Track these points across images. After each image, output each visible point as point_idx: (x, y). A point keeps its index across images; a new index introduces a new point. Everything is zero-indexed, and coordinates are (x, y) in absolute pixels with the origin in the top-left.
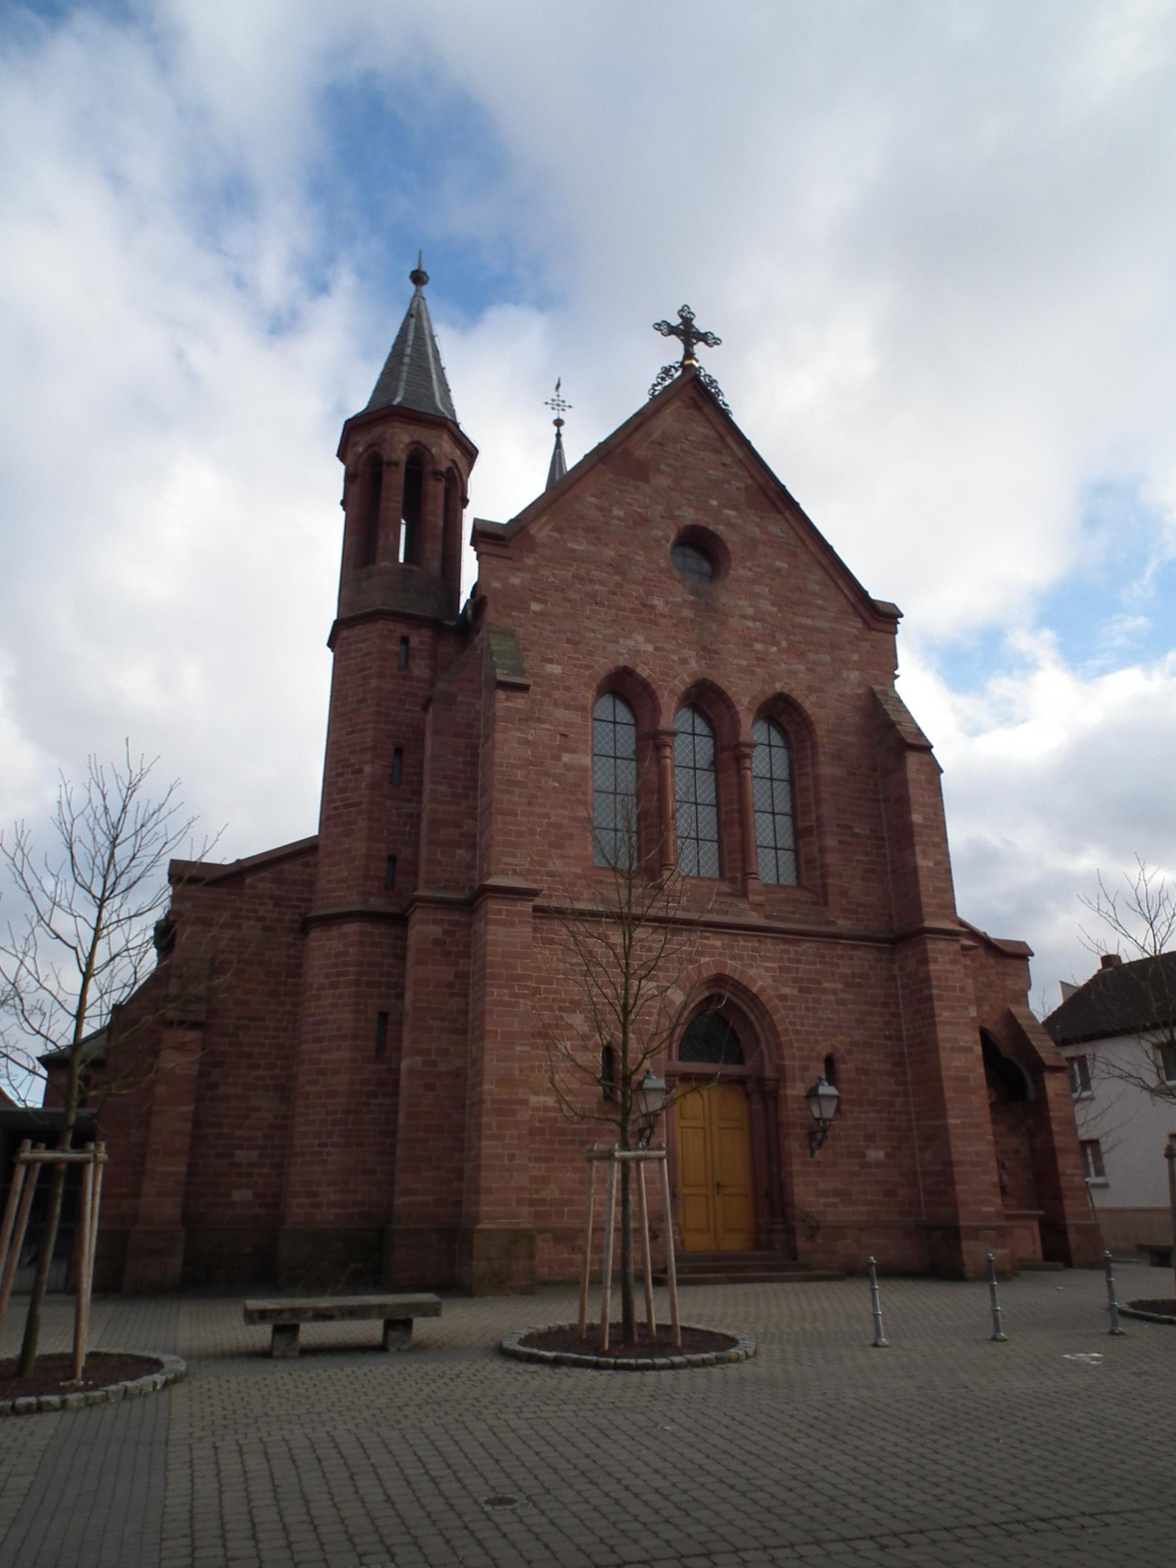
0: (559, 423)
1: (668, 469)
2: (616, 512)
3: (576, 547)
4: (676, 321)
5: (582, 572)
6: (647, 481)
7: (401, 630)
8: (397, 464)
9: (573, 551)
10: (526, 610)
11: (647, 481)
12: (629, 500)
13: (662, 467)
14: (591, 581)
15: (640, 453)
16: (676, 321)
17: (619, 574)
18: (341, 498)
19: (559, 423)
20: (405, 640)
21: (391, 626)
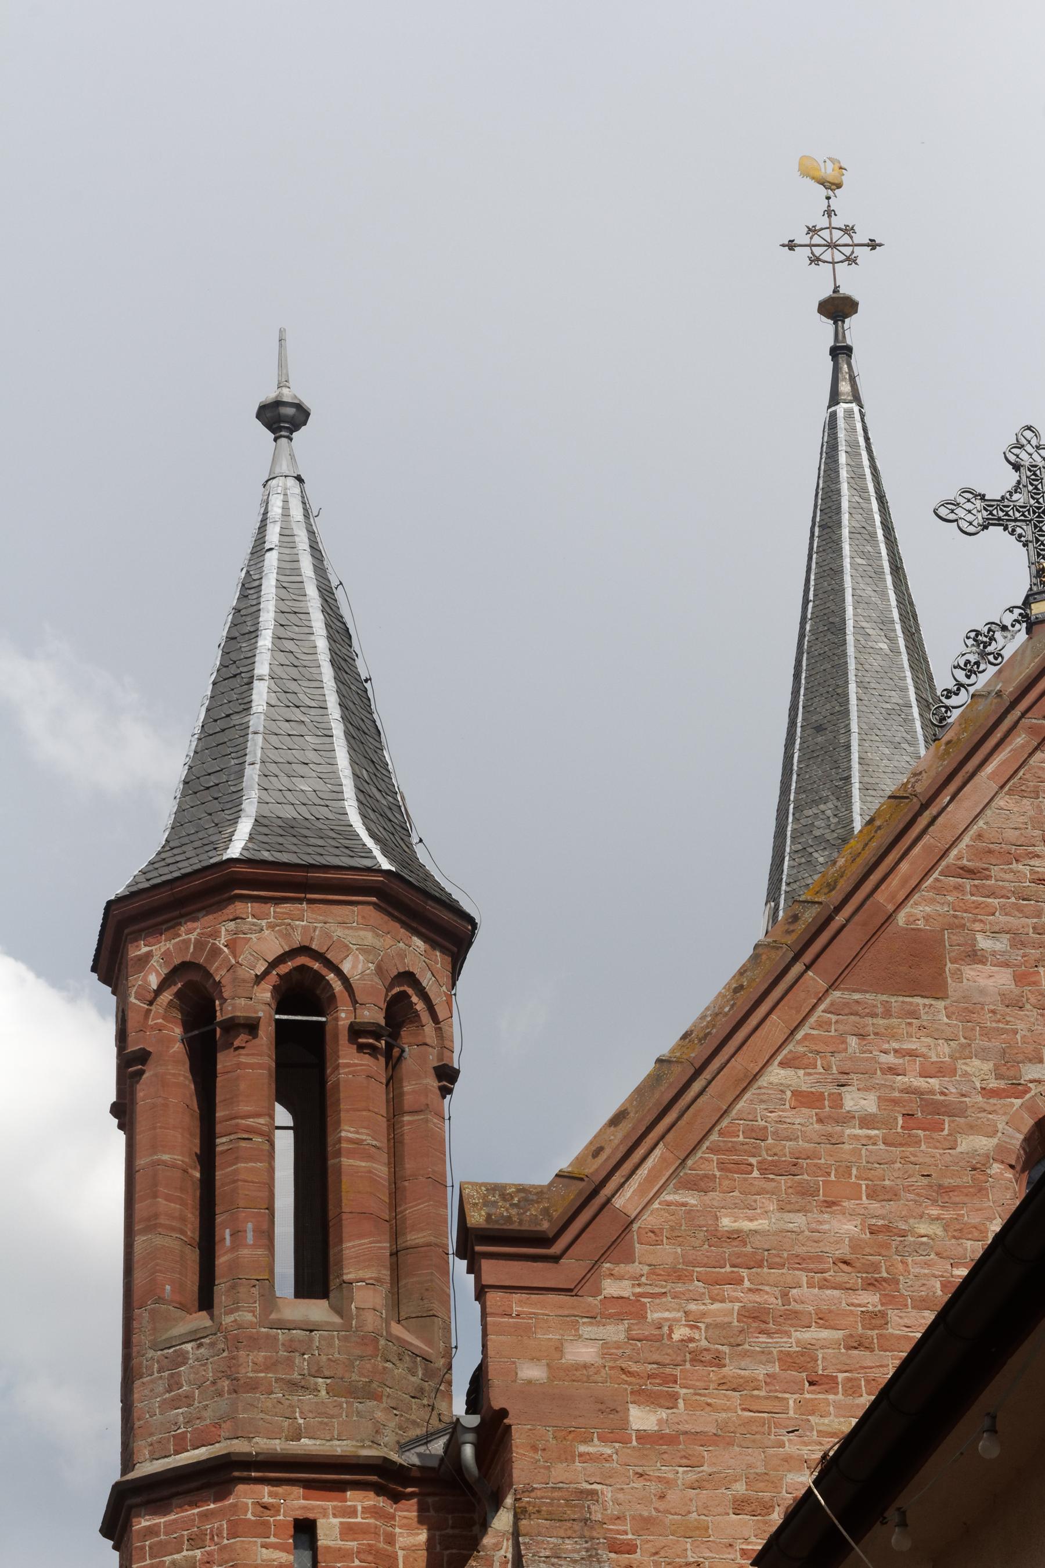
0: (838, 308)
1: (1001, 945)
2: (859, 1101)
3: (747, 1225)
4: (999, 481)
5: (770, 1299)
6: (935, 989)
7: (295, 1502)
8: (251, 1027)
9: (736, 1237)
10: (618, 1433)
11: (935, 989)
12: (890, 1059)
13: (983, 943)
14: (794, 1318)
15: (919, 913)
16: (999, 481)
17: (870, 1285)
18: (113, 1098)
19: (838, 308)
20: (305, 1530)
21: (266, 1493)
